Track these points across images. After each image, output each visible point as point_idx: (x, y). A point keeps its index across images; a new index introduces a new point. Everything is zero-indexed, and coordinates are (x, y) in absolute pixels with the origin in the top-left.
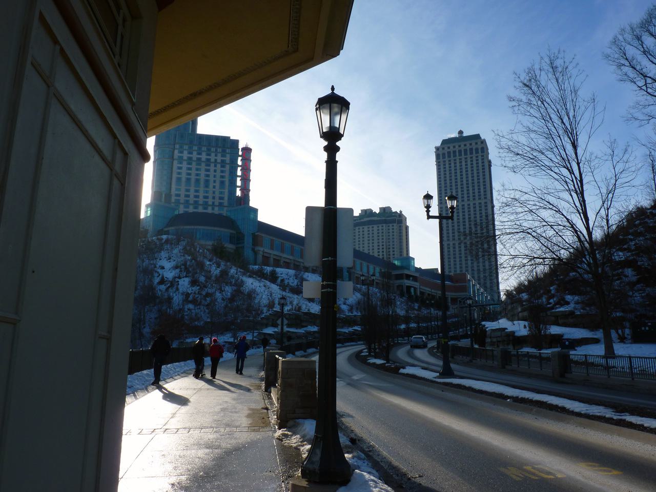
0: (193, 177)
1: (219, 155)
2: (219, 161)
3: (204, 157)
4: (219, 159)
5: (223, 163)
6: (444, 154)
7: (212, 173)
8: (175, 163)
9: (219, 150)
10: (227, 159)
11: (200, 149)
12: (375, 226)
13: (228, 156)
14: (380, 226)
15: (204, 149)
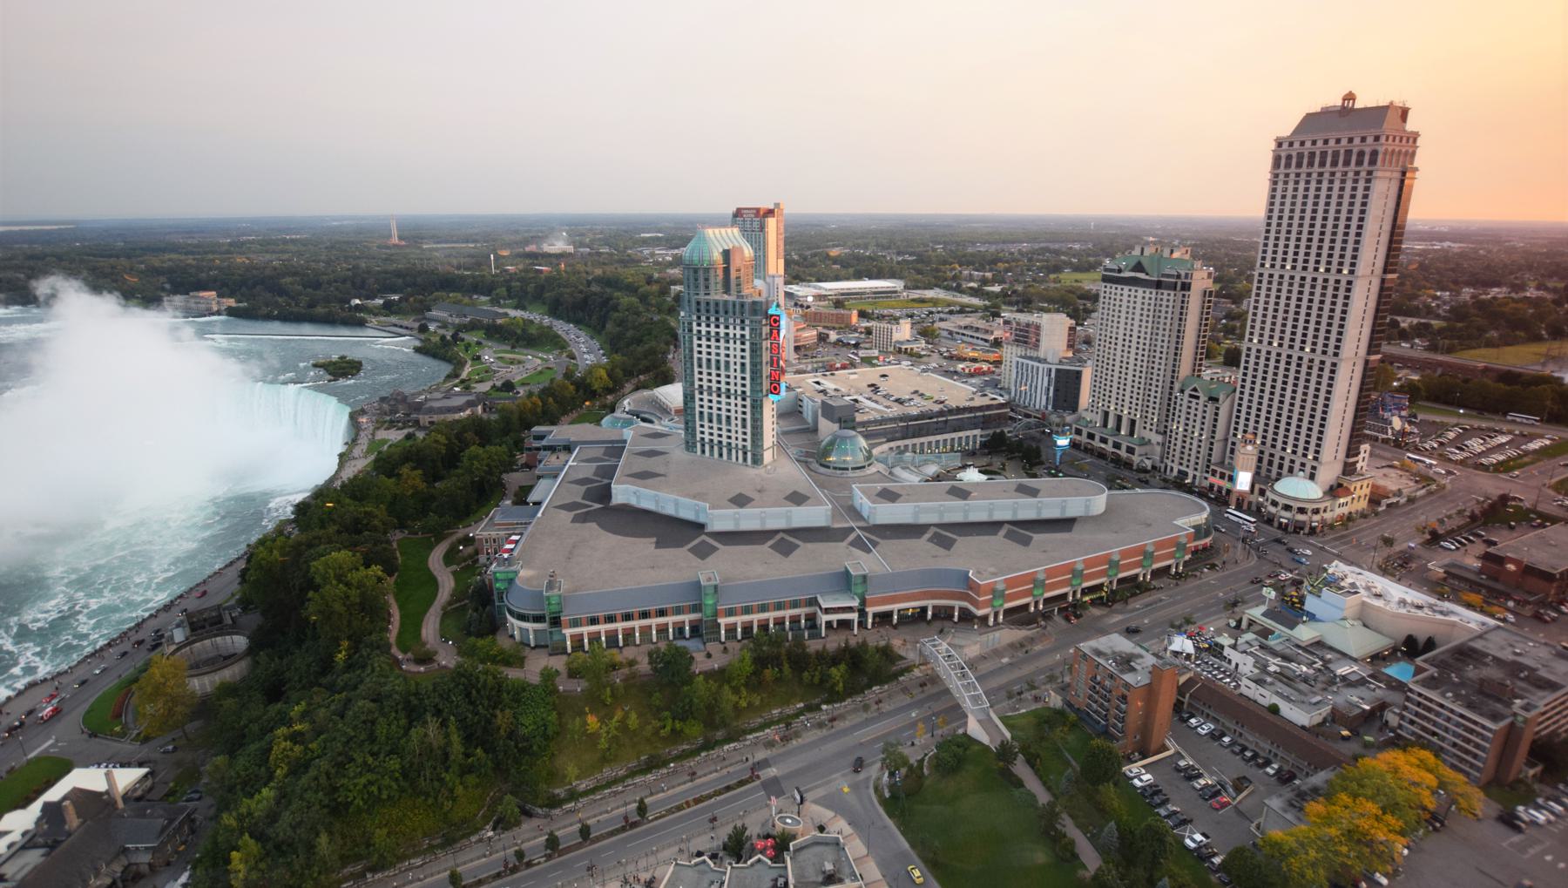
3: (722, 330)
4: (738, 332)
6: (1289, 157)
10: (747, 332)
12: (1140, 290)
13: (747, 329)
14: (1148, 291)
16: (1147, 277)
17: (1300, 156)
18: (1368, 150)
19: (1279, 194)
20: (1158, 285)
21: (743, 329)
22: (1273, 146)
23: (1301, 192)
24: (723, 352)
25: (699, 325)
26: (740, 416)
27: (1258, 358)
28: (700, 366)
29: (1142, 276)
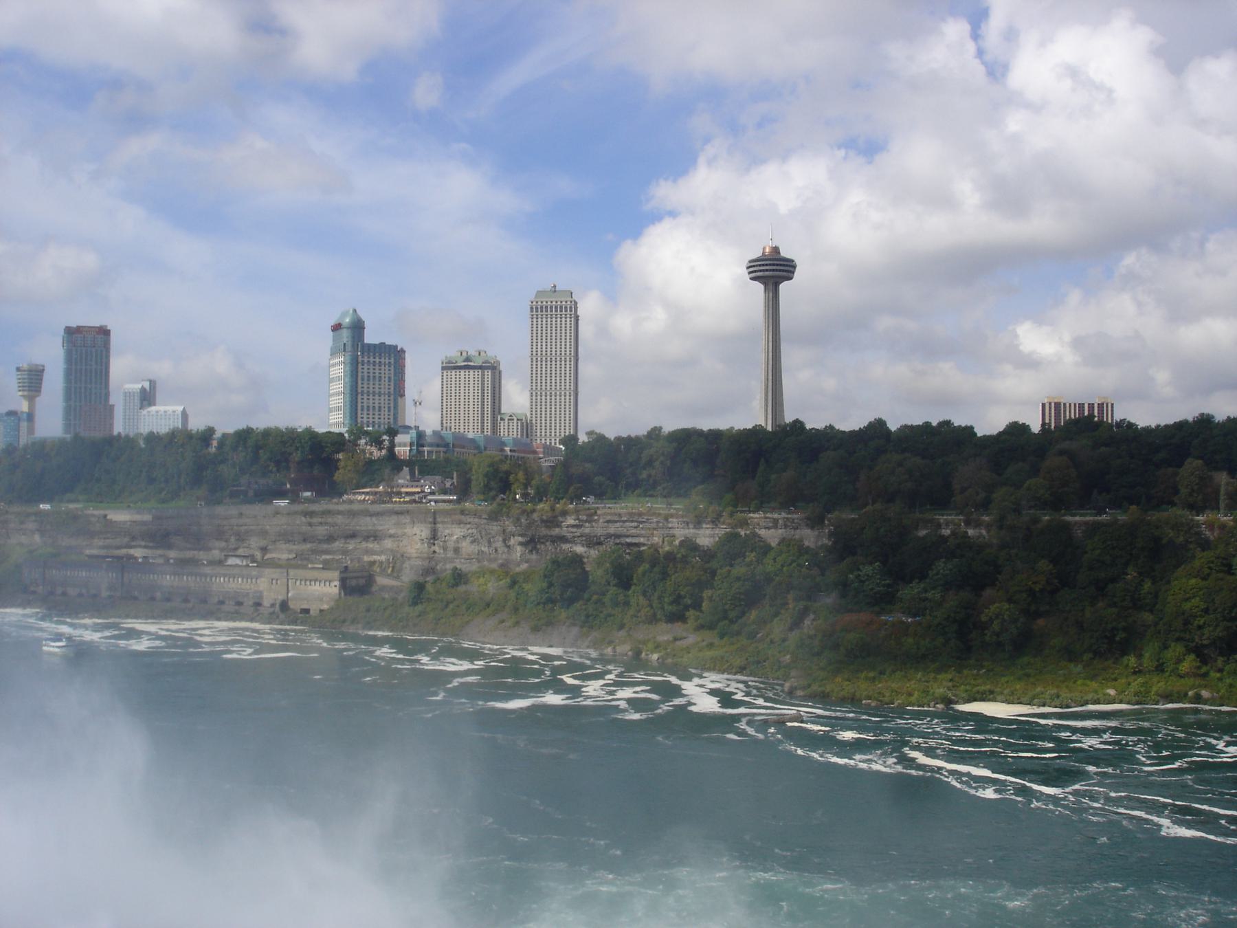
0: (371, 375)
2: (387, 363)
3: (377, 360)
6: (537, 308)
7: (383, 372)
8: (360, 365)
9: (387, 355)
10: (392, 361)
11: (374, 354)
12: (472, 372)
13: (393, 359)
15: (377, 354)
16: (475, 364)
19: (535, 323)
20: (480, 367)
21: (390, 359)
22: (530, 303)
24: (377, 371)
25: (363, 357)
26: (387, 406)
27: (536, 396)
28: (363, 380)
29: (470, 363)
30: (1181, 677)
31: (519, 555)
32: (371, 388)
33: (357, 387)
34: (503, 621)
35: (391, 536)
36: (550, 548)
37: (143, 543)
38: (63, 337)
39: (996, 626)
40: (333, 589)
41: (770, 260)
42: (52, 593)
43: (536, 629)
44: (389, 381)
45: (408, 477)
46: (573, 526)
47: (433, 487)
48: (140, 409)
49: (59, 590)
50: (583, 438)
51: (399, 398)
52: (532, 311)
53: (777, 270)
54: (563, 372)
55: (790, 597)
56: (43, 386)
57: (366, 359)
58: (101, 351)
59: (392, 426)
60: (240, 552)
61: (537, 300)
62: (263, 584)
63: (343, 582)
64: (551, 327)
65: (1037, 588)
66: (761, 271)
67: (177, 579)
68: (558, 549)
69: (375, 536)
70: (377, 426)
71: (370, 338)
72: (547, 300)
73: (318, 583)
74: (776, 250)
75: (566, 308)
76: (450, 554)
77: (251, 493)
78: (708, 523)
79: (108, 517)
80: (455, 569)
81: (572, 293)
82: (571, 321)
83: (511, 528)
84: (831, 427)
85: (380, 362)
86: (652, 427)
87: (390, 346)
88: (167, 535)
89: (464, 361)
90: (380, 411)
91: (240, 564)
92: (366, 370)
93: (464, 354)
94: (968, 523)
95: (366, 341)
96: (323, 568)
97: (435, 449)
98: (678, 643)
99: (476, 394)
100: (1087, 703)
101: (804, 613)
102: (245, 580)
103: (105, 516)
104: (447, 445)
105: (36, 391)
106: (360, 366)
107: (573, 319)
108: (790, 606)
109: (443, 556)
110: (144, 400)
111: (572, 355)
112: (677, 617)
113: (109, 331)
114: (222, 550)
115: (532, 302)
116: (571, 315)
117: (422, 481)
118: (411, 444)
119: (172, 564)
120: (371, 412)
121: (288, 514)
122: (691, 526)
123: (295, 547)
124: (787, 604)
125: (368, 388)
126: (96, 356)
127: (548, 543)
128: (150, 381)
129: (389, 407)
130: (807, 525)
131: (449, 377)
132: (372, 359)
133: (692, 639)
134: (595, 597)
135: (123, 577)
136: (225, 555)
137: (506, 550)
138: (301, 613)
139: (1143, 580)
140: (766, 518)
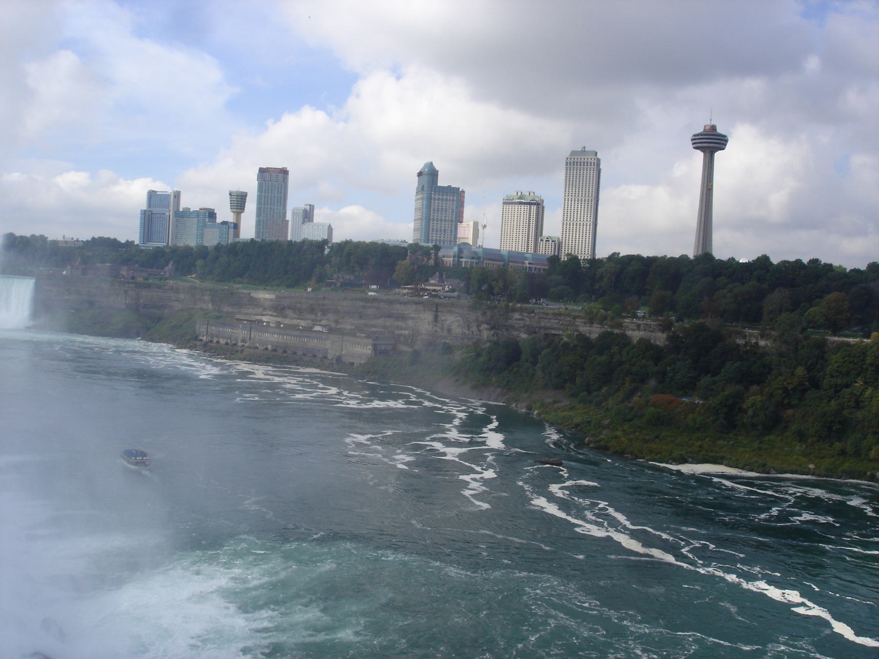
0: (440, 207)
1: (451, 196)
2: (451, 199)
4: (451, 198)
5: (453, 200)
6: (570, 163)
10: (455, 198)
12: (523, 206)
13: (455, 197)
14: (526, 206)
17: (574, 162)
18: (593, 162)
20: (530, 204)
22: (566, 159)
23: (575, 173)
24: (444, 205)
25: (435, 195)
26: (449, 229)
28: (434, 211)
30: (871, 461)
31: (486, 336)
32: (440, 216)
33: (430, 215)
34: (457, 380)
35: (412, 318)
36: (505, 334)
37: (270, 313)
38: (258, 174)
39: (750, 413)
40: (368, 350)
41: (709, 135)
42: (211, 341)
43: (474, 388)
44: (452, 212)
45: (437, 279)
46: (519, 320)
47: (450, 287)
48: (303, 224)
49: (215, 340)
50: (564, 258)
51: (459, 223)
52: (567, 165)
53: (711, 143)
54: (569, 208)
55: (627, 379)
56: (246, 206)
57: (437, 197)
58: (282, 184)
59: (438, 243)
60: (323, 322)
61: (571, 157)
62: (328, 344)
63: (375, 347)
64: (580, 177)
65: (790, 387)
66: (700, 143)
67: (280, 337)
68: (511, 334)
69: (402, 317)
70: (442, 242)
71: (442, 182)
72: (578, 157)
73: (359, 347)
74: (713, 128)
75: (591, 163)
76: (445, 333)
77: (338, 284)
78: (598, 324)
79: (251, 295)
80: (445, 343)
81: (596, 154)
82: (593, 173)
83: (481, 318)
84: (733, 259)
85: (446, 199)
86: (613, 252)
87: (454, 188)
88: (283, 309)
89: (518, 199)
90: (445, 232)
91: (321, 330)
92: (436, 204)
93: (519, 194)
94: (762, 336)
95: (439, 184)
96: (366, 337)
97: (470, 260)
98: (556, 405)
99: (525, 222)
100: (786, 472)
101: (632, 393)
102: (318, 341)
103: (250, 294)
104: (479, 258)
105: (241, 209)
106: (433, 201)
107: (595, 171)
108: (626, 386)
109: (441, 334)
110: (306, 218)
111: (593, 196)
112: (559, 387)
113: (288, 171)
114: (313, 320)
115: (567, 159)
116: (594, 168)
117: (445, 282)
118: (454, 257)
119: (301, 326)
120: (438, 233)
121: (352, 300)
122: (588, 325)
123: (355, 322)
124: (624, 384)
125: (438, 216)
126: (278, 187)
127: (504, 330)
128: (310, 205)
129: (451, 230)
130: (660, 329)
131: (507, 209)
132: (441, 197)
133: (566, 402)
134: (515, 369)
135: (250, 334)
136: (313, 324)
137: (479, 333)
138: (349, 365)
139: (867, 388)
140: (633, 323)
